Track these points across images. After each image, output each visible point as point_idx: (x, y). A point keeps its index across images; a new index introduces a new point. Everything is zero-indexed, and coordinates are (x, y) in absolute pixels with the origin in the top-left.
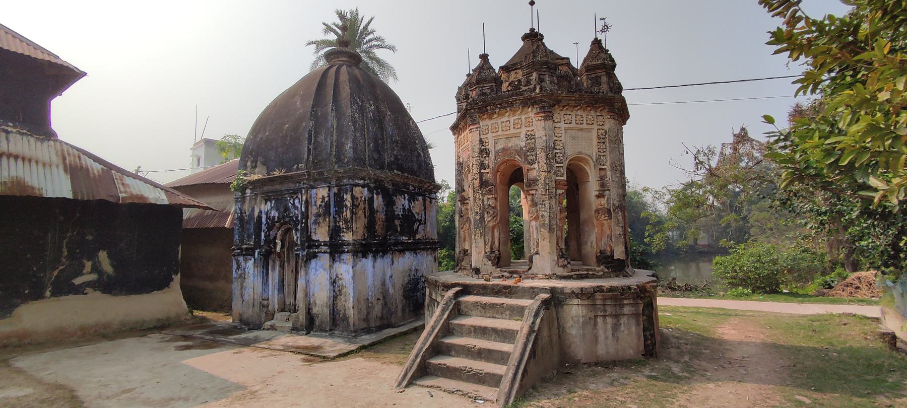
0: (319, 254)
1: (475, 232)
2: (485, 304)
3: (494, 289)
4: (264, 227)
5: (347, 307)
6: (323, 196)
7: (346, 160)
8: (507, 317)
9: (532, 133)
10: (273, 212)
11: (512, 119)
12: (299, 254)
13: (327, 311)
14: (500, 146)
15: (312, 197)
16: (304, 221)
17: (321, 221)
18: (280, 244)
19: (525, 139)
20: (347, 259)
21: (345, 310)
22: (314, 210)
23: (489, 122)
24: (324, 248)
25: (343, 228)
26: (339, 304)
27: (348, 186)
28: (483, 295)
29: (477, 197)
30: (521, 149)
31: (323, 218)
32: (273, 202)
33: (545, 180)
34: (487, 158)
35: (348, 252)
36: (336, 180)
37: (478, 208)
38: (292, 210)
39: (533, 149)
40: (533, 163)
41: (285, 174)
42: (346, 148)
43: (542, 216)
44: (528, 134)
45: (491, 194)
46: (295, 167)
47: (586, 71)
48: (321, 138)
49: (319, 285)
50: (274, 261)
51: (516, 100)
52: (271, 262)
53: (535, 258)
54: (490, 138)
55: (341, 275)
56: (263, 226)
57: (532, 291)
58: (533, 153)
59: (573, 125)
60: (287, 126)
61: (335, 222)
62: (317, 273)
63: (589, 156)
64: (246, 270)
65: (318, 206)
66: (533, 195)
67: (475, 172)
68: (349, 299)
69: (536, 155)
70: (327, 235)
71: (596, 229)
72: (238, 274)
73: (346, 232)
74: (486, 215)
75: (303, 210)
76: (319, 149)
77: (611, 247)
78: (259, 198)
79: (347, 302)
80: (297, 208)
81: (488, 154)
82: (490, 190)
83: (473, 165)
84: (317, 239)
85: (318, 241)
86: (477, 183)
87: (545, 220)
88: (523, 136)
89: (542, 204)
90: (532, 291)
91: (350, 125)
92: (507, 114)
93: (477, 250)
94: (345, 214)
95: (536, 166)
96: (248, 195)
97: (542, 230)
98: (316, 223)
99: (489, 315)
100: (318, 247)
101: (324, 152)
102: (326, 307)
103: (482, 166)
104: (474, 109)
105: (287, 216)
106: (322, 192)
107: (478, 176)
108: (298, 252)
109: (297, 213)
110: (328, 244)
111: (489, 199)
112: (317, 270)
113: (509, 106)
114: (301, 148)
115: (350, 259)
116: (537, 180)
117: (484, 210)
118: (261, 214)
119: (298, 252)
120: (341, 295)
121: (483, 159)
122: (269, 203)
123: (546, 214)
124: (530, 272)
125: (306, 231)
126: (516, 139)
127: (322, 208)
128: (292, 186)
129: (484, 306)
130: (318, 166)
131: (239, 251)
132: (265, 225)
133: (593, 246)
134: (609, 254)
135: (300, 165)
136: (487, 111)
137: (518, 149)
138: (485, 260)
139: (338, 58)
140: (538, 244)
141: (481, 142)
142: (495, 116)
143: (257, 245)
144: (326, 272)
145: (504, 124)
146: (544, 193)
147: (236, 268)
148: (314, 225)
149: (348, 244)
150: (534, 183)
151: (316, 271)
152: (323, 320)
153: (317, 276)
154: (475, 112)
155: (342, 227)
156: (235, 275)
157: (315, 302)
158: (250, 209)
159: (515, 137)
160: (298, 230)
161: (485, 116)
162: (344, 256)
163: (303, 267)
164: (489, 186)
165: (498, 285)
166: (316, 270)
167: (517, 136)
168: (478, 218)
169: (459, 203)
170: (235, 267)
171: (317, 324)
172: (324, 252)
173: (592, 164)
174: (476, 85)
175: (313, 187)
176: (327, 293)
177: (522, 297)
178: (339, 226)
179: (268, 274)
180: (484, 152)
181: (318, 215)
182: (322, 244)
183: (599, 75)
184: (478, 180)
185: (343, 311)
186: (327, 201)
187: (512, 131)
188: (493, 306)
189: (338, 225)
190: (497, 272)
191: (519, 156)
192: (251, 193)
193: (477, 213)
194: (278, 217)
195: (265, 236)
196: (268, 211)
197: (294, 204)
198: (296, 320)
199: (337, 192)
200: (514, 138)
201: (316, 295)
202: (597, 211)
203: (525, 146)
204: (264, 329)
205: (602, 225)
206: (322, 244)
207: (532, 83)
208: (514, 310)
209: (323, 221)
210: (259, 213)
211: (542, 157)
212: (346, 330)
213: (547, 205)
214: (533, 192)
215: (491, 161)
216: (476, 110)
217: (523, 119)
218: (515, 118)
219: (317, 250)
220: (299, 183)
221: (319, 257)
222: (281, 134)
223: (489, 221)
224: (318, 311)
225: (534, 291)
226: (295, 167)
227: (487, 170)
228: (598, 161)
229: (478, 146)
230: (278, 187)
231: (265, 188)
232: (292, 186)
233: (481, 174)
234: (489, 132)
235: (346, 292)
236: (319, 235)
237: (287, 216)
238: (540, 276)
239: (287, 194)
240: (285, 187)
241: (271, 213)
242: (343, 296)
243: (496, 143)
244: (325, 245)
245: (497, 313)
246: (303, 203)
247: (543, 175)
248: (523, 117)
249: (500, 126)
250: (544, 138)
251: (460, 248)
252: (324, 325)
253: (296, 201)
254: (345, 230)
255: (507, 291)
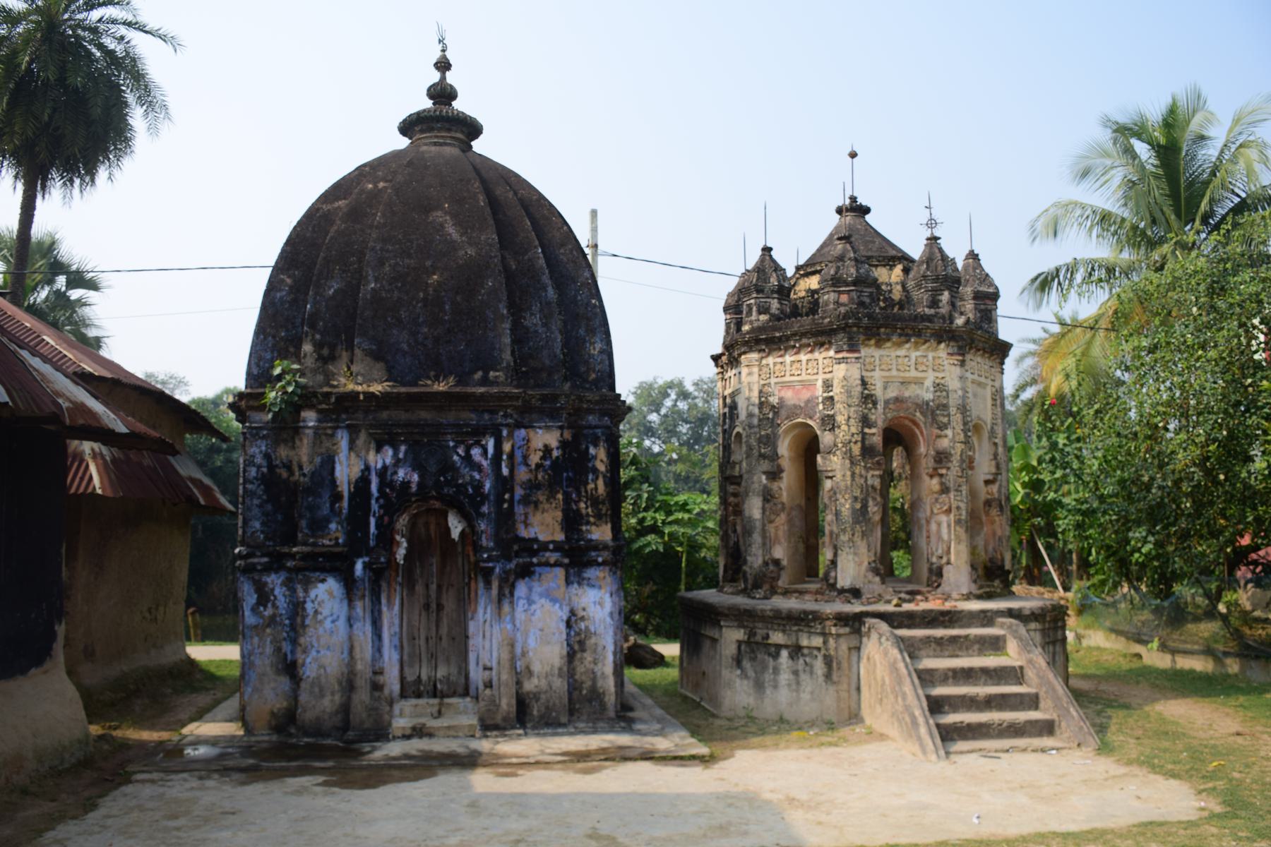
0: (537, 569)
1: (852, 529)
2: (942, 638)
3: (925, 618)
4: (375, 506)
5: (599, 674)
6: (546, 446)
7: (593, 376)
8: (976, 653)
9: (942, 381)
10: (401, 473)
11: (914, 354)
12: (493, 569)
13: (560, 685)
14: (892, 394)
15: (517, 446)
16: (507, 496)
17: (542, 498)
18: (405, 545)
19: (932, 389)
20: (598, 577)
21: (594, 680)
22: (522, 474)
23: (877, 353)
24: (553, 557)
25: (588, 515)
26: (580, 669)
27: (599, 431)
28: (909, 627)
29: (857, 471)
30: (927, 404)
31: (547, 492)
32: (403, 448)
33: (961, 455)
34: (873, 411)
35: (604, 563)
36: (569, 414)
37: (859, 491)
38: (465, 471)
39: (945, 407)
40: (943, 427)
41: (458, 389)
42: (592, 352)
43: (958, 508)
44: (937, 381)
45: (879, 469)
46: (479, 375)
47: (975, 298)
48: (533, 320)
49: (539, 633)
50: (389, 585)
51: (928, 328)
52: (384, 585)
53: (946, 570)
54: (877, 378)
55: (584, 609)
56: (373, 502)
57: (982, 615)
58: (945, 413)
59: (975, 377)
60: (435, 277)
61: (567, 499)
62: (534, 607)
63: (986, 423)
64: (309, 606)
65: (533, 467)
66: (941, 476)
67: (853, 430)
68: (605, 658)
69: (949, 415)
70: (558, 528)
71: (985, 529)
72: (263, 617)
73: (594, 524)
74: (871, 503)
75: (505, 471)
76: (531, 344)
77: (1001, 555)
78: (362, 438)
79: (600, 665)
80: (479, 468)
81: (875, 403)
82: (878, 463)
83: (849, 418)
84: (532, 535)
85: (536, 540)
86: (856, 449)
87: (960, 515)
88: (928, 383)
89: (957, 490)
90: (982, 615)
91: (595, 305)
92: (907, 346)
93: (856, 559)
94: (591, 486)
95: (949, 432)
96: (311, 424)
97: (958, 528)
98: (526, 501)
99: (947, 653)
100: (534, 553)
101: (545, 352)
102: (560, 676)
103: (865, 421)
104: (859, 327)
105: (447, 483)
106: (546, 438)
107: (859, 438)
108: (491, 565)
109: (477, 477)
110: (566, 547)
111: (873, 476)
112: (534, 602)
113: (914, 335)
114: (491, 334)
115: (604, 578)
116: (951, 455)
117: (868, 494)
118: (369, 474)
119: (491, 565)
120: (583, 650)
121: (866, 411)
122: (389, 452)
123: (963, 505)
124: (939, 590)
125: (505, 520)
126: (916, 387)
127: (545, 471)
128: (472, 418)
129: (939, 642)
130: (532, 381)
131: (265, 560)
132: (377, 500)
133: (977, 552)
134: (1000, 563)
135: (492, 374)
136: (879, 334)
137: (919, 402)
138: (870, 575)
139: (449, 130)
140: (949, 548)
141: (864, 383)
142: (888, 344)
143: (357, 544)
144: (558, 605)
145: (900, 360)
146: (960, 474)
147: (254, 601)
148: (521, 507)
149: (606, 547)
150: (946, 457)
151: (530, 605)
152: (551, 704)
153: (533, 614)
154: (859, 333)
155: (584, 511)
156: (250, 618)
157: (528, 668)
158: (318, 460)
159: (915, 383)
160: (482, 515)
161: (873, 342)
162: (591, 573)
163: (508, 595)
164: (876, 456)
165: (931, 611)
166: (530, 602)
167: (919, 382)
168: (858, 506)
169: (764, 477)
170: (249, 597)
171: (535, 713)
172: (556, 564)
173: (986, 435)
174: (847, 285)
175: (519, 425)
176: (562, 647)
177: (969, 626)
178: (578, 510)
179: (380, 612)
180: (868, 399)
181: (532, 486)
182: (551, 546)
183: (989, 307)
184: (859, 444)
185: (589, 683)
186: (557, 457)
187: (913, 373)
188: (954, 640)
189: (574, 507)
190: (888, 591)
191: (921, 413)
192: (319, 421)
193: (856, 498)
194: (420, 484)
195: (377, 526)
196: (385, 467)
197: (468, 458)
198: (489, 710)
199: (570, 439)
200: (913, 385)
201: (531, 654)
202: (988, 503)
203: (933, 401)
204: (395, 738)
205: (993, 522)
206: (551, 546)
207: (941, 305)
208: (985, 642)
209: (548, 500)
210: (362, 471)
211: (957, 419)
212: (597, 719)
213: (964, 492)
214: (944, 471)
215: (879, 416)
216: (861, 330)
217: (930, 358)
218: (918, 353)
219: (535, 560)
220: (493, 412)
221: (537, 575)
222: (421, 295)
223: (874, 513)
224: (536, 687)
225: (986, 616)
226: (479, 375)
227: (873, 430)
228: (992, 433)
229: (859, 389)
230: (425, 415)
231: (385, 415)
232: (472, 418)
233: (864, 434)
234: (877, 368)
235: (596, 644)
236: (537, 529)
237: (447, 483)
238: (957, 597)
239: (451, 434)
240: (450, 417)
241: (396, 473)
242: (588, 652)
243: (885, 388)
244: (555, 550)
245: (960, 649)
246: (505, 457)
247: (959, 447)
248: (931, 355)
249: (894, 362)
250: (960, 393)
251: (764, 556)
252: (554, 714)
253: (476, 452)
254: (592, 520)
255: (947, 618)
